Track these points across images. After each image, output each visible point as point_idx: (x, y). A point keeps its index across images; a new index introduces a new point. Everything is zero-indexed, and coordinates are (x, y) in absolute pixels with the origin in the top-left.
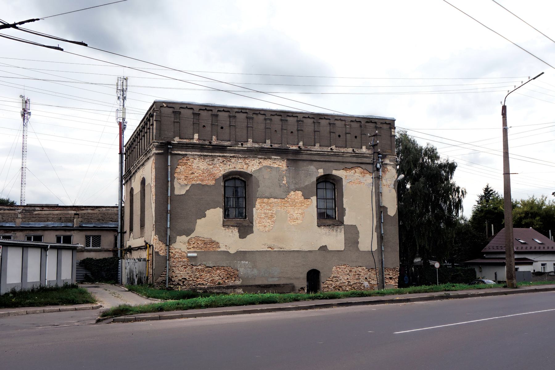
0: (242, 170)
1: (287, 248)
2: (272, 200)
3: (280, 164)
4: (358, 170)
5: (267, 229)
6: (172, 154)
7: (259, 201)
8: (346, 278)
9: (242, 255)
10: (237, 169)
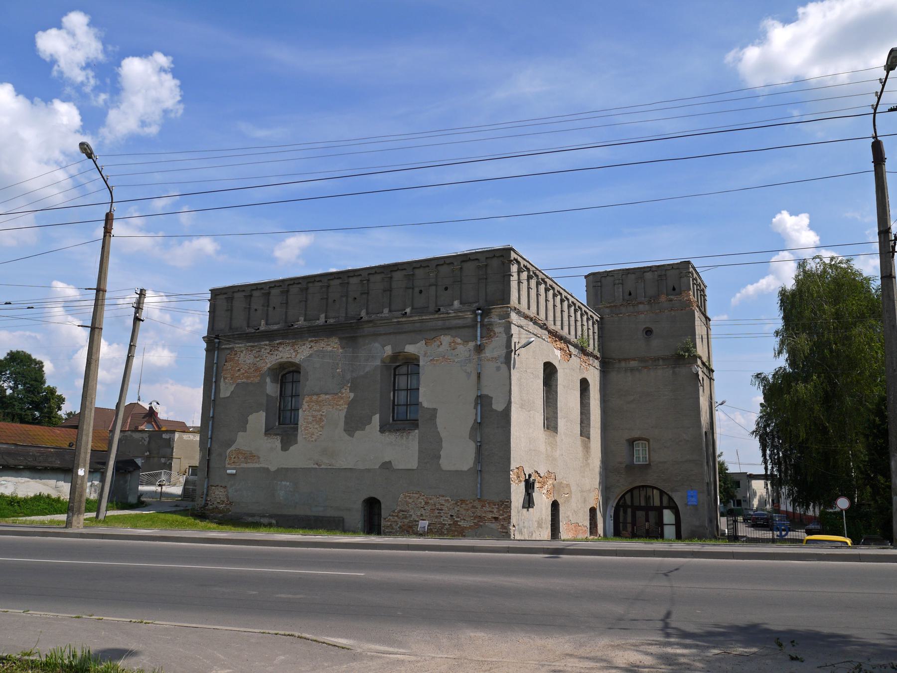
0: (290, 360)
1: (337, 466)
2: (323, 397)
3: (332, 346)
4: (446, 339)
5: (315, 437)
6: (218, 348)
7: (307, 399)
8: (419, 514)
9: (283, 473)
10: (284, 360)
